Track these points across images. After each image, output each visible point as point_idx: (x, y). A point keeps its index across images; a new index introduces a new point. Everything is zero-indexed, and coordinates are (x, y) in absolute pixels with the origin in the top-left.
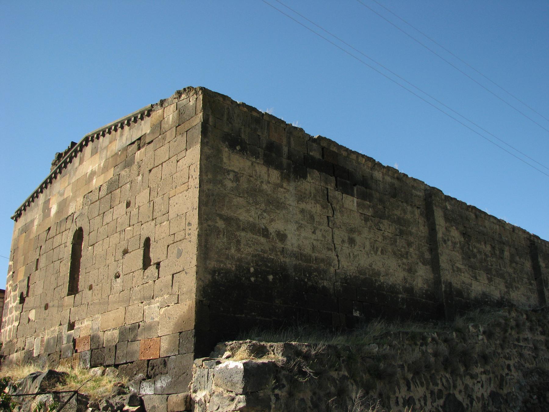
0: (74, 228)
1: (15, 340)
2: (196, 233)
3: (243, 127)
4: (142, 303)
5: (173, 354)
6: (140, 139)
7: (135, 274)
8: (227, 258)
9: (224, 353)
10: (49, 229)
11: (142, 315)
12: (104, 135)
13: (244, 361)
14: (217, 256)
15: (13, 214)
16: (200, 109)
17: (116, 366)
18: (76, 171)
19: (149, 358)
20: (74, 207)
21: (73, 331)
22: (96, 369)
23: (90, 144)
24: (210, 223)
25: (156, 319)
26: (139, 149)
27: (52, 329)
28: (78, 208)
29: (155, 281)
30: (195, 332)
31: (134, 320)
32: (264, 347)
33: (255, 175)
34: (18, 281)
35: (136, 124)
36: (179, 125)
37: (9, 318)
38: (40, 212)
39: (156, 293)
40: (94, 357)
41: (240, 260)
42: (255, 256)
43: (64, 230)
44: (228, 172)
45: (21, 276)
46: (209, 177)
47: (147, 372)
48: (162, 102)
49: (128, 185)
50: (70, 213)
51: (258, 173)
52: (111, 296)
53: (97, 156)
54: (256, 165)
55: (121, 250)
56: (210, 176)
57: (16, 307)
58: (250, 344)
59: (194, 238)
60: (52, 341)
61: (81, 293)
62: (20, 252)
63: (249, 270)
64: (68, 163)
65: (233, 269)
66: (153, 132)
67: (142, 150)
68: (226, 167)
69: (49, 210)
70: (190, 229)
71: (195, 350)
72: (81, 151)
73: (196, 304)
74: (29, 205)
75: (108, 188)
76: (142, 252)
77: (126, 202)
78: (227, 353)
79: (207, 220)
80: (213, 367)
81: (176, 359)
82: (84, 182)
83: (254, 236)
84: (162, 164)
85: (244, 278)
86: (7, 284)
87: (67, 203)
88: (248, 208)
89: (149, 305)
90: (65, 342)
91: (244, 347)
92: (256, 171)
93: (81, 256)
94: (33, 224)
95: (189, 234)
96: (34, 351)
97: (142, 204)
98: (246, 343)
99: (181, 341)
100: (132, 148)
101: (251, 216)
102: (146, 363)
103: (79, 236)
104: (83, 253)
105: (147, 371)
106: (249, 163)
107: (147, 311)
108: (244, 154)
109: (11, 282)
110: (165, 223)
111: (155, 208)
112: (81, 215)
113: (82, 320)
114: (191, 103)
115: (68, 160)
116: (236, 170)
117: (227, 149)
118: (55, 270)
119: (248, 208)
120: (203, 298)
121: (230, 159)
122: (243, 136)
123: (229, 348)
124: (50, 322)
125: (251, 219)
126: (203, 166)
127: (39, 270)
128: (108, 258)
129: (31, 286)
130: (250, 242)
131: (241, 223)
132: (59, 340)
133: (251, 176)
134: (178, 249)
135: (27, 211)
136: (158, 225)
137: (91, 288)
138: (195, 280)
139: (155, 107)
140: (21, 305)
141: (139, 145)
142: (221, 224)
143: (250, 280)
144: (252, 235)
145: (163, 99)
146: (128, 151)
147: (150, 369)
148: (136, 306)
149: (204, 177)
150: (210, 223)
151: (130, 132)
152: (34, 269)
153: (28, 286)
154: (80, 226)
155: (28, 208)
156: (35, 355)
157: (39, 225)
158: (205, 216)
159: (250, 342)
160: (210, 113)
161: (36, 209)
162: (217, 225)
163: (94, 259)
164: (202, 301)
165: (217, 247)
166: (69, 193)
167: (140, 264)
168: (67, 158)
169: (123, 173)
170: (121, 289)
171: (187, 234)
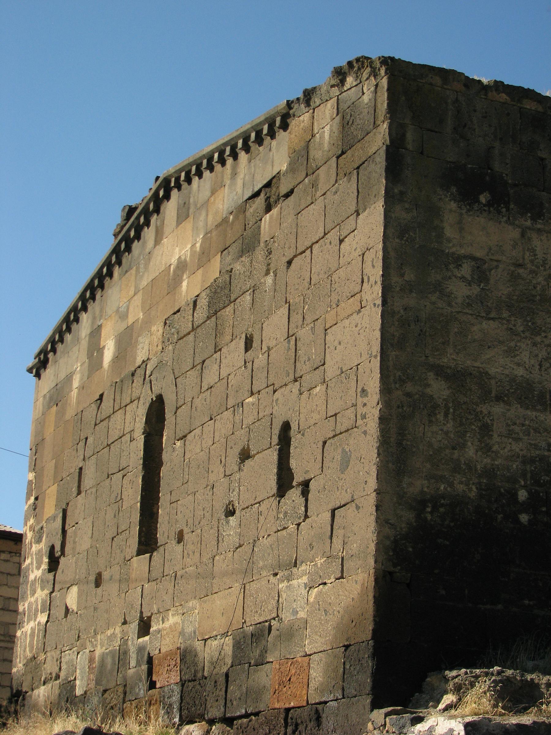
0: (147, 397)
1: (42, 657)
2: (376, 413)
3: (497, 144)
4: (276, 574)
5: (331, 697)
6: (268, 185)
7: (263, 507)
8: (456, 469)
9: (442, 697)
11: (274, 602)
12: (199, 174)
13: (469, 719)
14: (428, 466)
15: (31, 361)
16: (384, 112)
17: (229, 721)
18: (149, 259)
19: (287, 706)
20: (146, 348)
21: (147, 638)
22: (191, 727)
23: (174, 193)
24: (409, 387)
25: (302, 615)
26: (268, 208)
27: (109, 632)
28: (155, 348)
29: (298, 525)
30: (374, 647)
31: (260, 615)
32: (533, 686)
33: (532, 262)
34: (45, 518)
35: (261, 148)
36: (343, 153)
37: (30, 604)
38: (83, 356)
39: (301, 551)
40: (187, 699)
41: (489, 473)
42: (532, 461)
43: (128, 401)
44: (458, 260)
45: (50, 508)
46: (407, 278)
48: (308, 96)
49: (248, 297)
50: (139, 361)
51: (540, 255)
52: (217, 558)
53: (188, 225)
54: (534, 235)
56: (410, 275)
57: (42, 581)
58: (498, 678)
59: (372, 425)
60: (109, 660)
61: (162, 549)
62: (48, 451)
63: (514, 495)
64: (132, 241)
65: (473, 493)
66: (292, 168)
67: (275, 211)
68: (454, 249)
70: (365, 405)
71: (374, 688)
72: (157, 210)
73: (376, 580)
74: (61, 340)
75: (209, 302)
77: (243, 336)
78: (449, 699)
79: (402, 381)
80: (405, 731)
81: (338, 708)
82: (166, 286)
83: (529, 413)
84: (311, 247)
85: (500, 517)
86: (26, 524)
87: (135, 335)
88: (512, 344)
89: (289, 581)
90: (133, 663)
91: (483, 686)
92: (533, 251)
93: (162, 464)
94: (71, 384)
95: (364, 417)
96: (78, 682)
97: (274, 342)
98: (487, 674)
99: (348, 667)
100: (254, 206)
101: (518, 365)
102: (282, 716)
106: (514, 233)
107: (284, 595)
108: (499, 212)
109: (32, 521)
110: (318, 389)
111: (300, 353)
112: (160, 364)
113: (163, 613)
114: (366, 98)
115: (132, 233)
116: (478, 254)
117: (453, 205)
118: (113, 496)
119: (512, 344)
120: (395, 565)
121: (461, 229)
122: (497, 166)
123: (451, 685)
124: (106, 616)
125: (520, 372)
126: (392, 254)
127: (83, 494)
128: (211, 467)
129: (70, 532)
130: (517, 429)
131: (493, 382)
132: (122, 656)
133: (520, 266)
134: (344, 450)
135: (58, 353)
136: (306, 394)
137: (180, 538)
138: (373, 525)
139: (296, 106)
140: (51, 576)
141: (268, 199)
142: (438, 389)
143: (517, 521)
144: (522, 411)
145: (309, 87)
146: (248, 214)
147: (290, 729)
148: (264, 582)
149: (395, 279)
150: (409, 387)
151: (250, 168)
152: (75, 490)
153: (64, 532)
154: (158, 392)
155: (59, 347)
156: (79, 692)
157: (82, 388)
158: (399, 373)
159: (499, 673)
160: (407, 121)
161: (75, 349)
162: (428, 391)
163: (186, 469)
164: (391, 573)
165: (430, 445)
166: (136, 314)
167: (272, 485)
168: (129, 230)
169: (238, 267)
171: (359, 417)
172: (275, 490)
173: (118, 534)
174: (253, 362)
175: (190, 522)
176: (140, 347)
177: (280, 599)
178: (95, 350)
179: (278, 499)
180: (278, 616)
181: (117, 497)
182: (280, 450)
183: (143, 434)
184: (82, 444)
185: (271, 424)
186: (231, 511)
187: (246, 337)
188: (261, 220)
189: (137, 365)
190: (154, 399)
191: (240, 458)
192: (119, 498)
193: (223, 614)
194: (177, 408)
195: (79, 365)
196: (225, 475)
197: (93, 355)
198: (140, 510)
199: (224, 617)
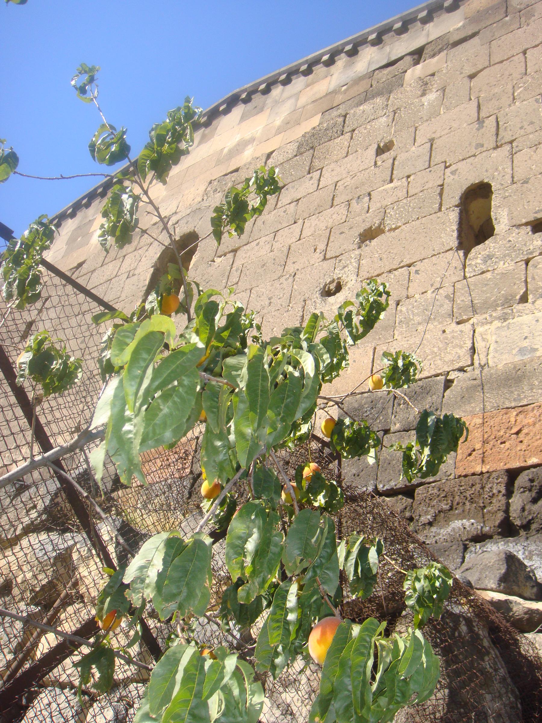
10: (80, 265)
47: (507, 511)
76: (454, 216)
105: (508, 505)
107: (492, 339)
172: (454, 243)
174: (394, 159)
177: (480, 345)
180: (472, 364)
183: (152, 267)
187: (379, 146)
188: (406, 71)
196: (325, 259)
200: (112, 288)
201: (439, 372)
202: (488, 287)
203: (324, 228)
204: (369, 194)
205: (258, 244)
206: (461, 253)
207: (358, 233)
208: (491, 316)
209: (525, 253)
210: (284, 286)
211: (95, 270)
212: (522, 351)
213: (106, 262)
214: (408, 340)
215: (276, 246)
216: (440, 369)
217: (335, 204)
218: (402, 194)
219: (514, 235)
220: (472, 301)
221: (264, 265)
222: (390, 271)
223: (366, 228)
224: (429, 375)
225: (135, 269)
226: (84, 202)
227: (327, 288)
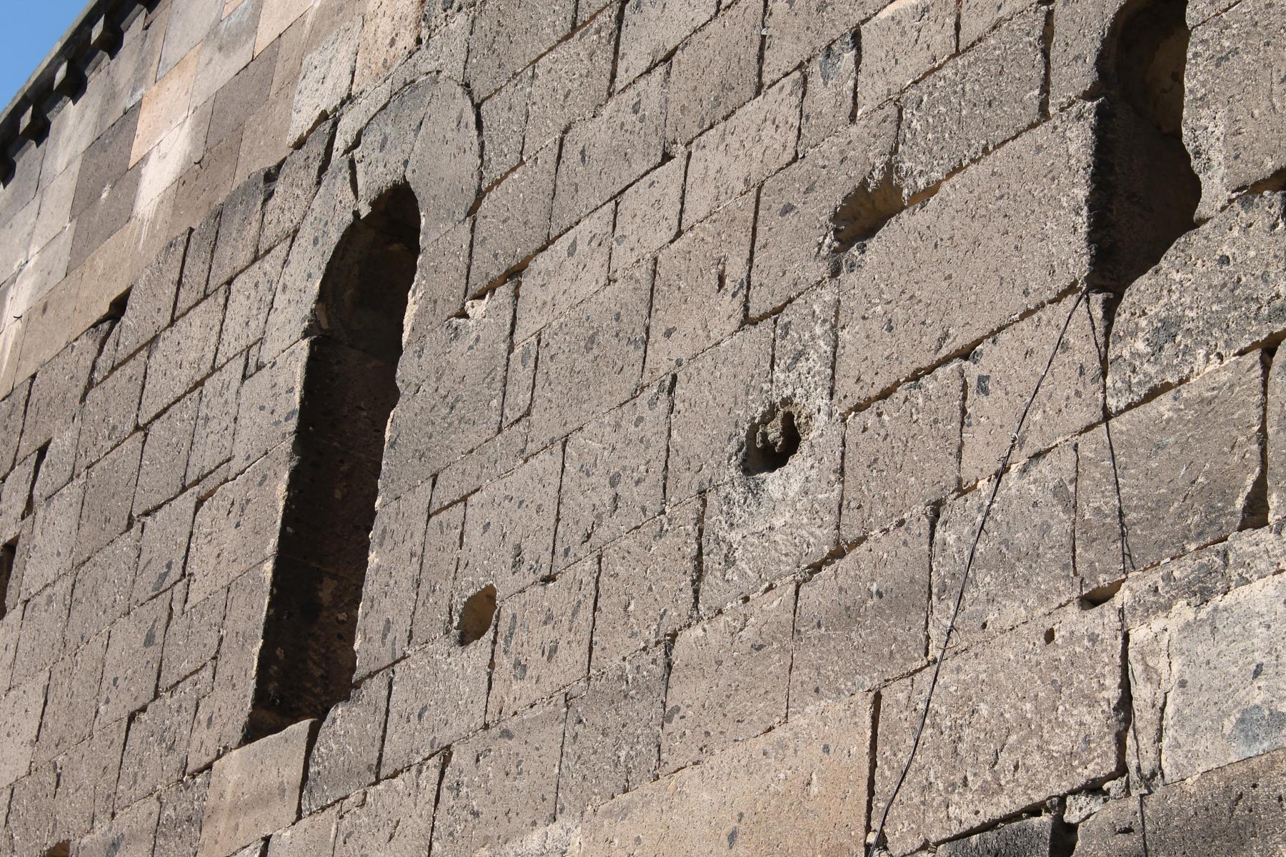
4: (1092, 600)
10: (119, 307)
11: (1097, 720)
43: (245, 256)
50: (302, 120)
55: (833, 196)
61: (376, 688)
69: (126, 177)
76: (1075, 140)
93: (392, 395)
103: (377, 256)
104: (407, 370)
137: (477, 618)
163: (522, 374)
170: (820, 540)
172: (1077, 264)
173: (157, 695)
175: (537, 549)
176: (308, 83)
177: (1142, 692)
178: (111, 164)
179: (1097, 299)
180: (1122, 769)
181: (163, 576)
182: (1100, 112)
183: (306, 334)
184: (24, 471)
185: (1047, 37)
186: (768, 446)
189: (291, 138)
190: (365, 211)
191: (836, 231)
192: (176, 572)
193: (732, 837)
194: (480, 195)
195: (34, 249)
196: (748, 321)
197: (94, 197)
198: (273, 584)
199: (740, 848)
200: (207, 419)
201: (1038, 797)
202: (1163, 455)
203: (740, 187)
204: (856, 36)
205: (572, 250)
206: (1097, 299)
207: (828, 212)
208: (1168, 578)
209: (1265, 311)
210: (648, 430)
211: (155, 339)
212: (1249, 723)
213: (182, 306)
214: (959, 669)
215: (623, 257)
216: (1038, 788)
217: (767, 79)
218: (941, 39)
219: (1235, 233)
220: (1121, 515)
221: (592, 340)
222: (916, 377)
223: (849, 187)
224: (1014, 809)
225: (261, 341)
226: (96, 32)
227: (759, 439)
